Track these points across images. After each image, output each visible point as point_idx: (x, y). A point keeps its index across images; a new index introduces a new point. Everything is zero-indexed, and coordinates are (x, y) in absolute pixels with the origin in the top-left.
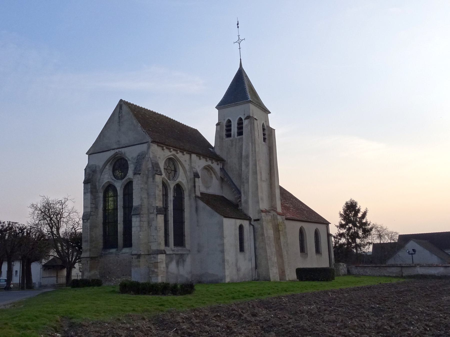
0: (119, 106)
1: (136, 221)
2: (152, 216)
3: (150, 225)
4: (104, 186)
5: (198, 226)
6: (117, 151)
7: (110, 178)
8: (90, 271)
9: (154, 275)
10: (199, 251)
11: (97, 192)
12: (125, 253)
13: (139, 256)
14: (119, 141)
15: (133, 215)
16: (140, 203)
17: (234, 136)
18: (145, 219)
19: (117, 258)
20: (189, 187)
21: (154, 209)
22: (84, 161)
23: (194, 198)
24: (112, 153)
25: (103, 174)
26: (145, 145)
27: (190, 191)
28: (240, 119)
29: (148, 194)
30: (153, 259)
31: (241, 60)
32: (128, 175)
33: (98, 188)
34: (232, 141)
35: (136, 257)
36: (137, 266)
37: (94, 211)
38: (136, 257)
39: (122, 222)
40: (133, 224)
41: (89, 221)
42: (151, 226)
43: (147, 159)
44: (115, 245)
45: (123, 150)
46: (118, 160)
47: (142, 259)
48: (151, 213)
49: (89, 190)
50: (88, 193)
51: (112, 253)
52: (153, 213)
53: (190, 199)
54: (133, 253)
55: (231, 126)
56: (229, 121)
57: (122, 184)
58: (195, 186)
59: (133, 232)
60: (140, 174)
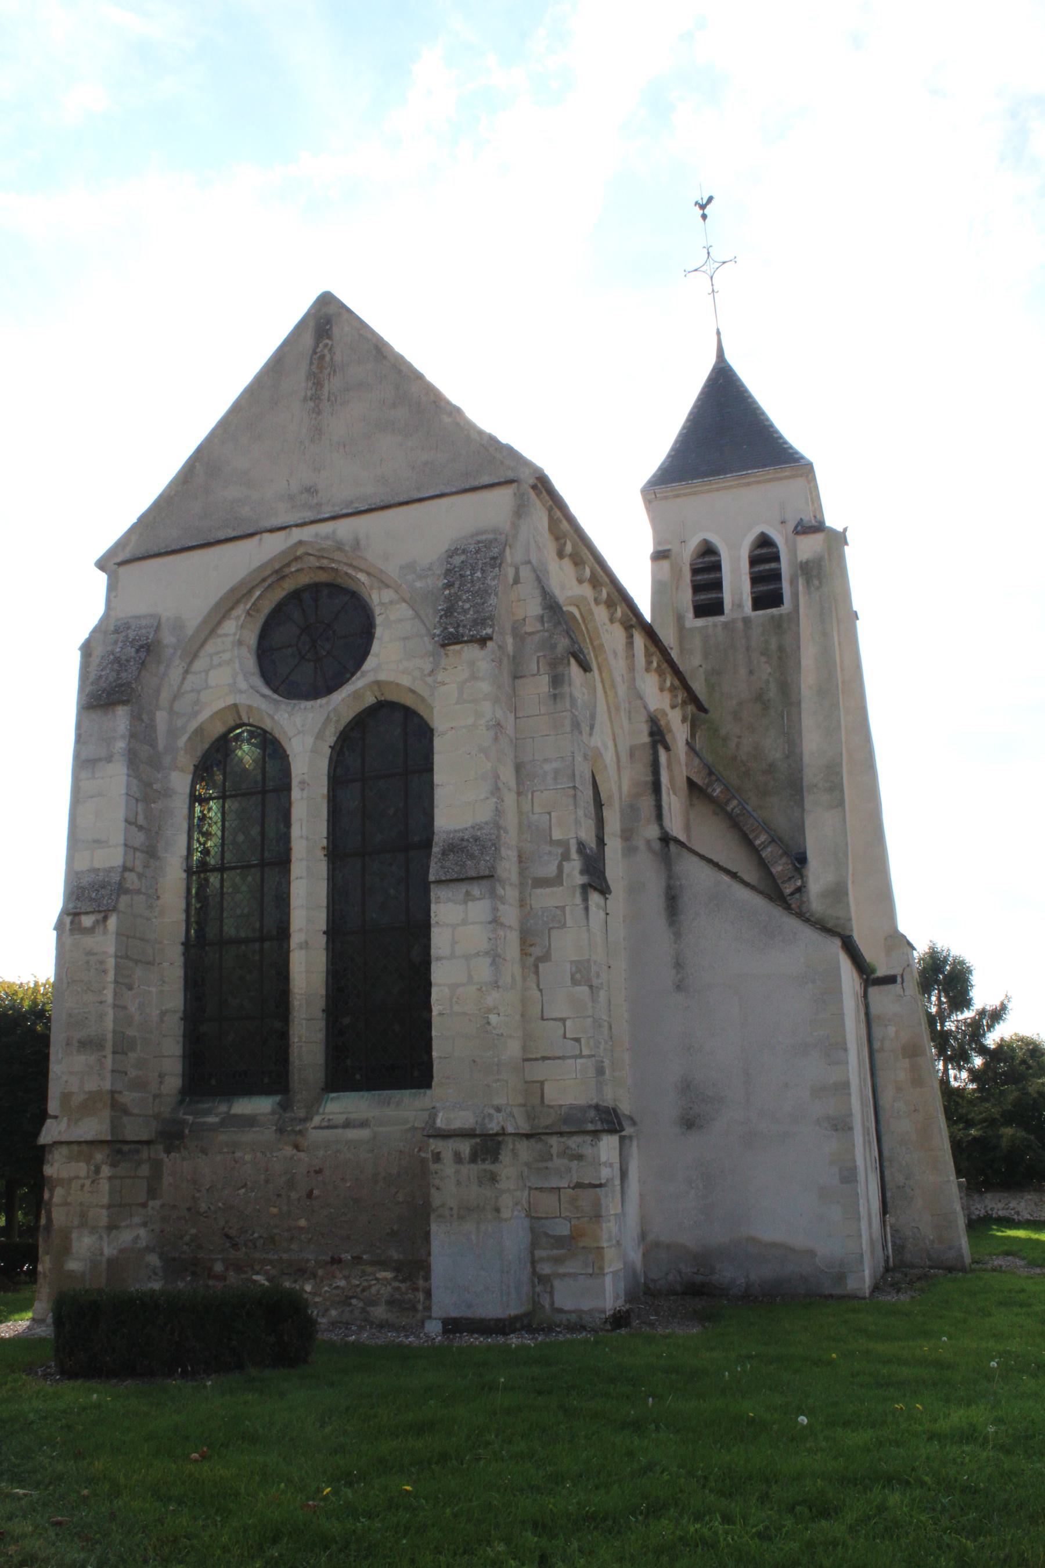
0: (312, 324)
1: (464, 922)
2: (546, 899)
3: (537, 951)
4: (199, 731)
5: (679, 987)
6: (298, 535)
7: (243, 685)
8: (112, 1227)
9: (570, 1267)
10: (689, 1123)
11: (155, 762)
12: (347, 1125)
13: (487, 1145)
14: (311, 490)
15: (439, 882)
16: (484, 814)
17: (740, 606)
18: (510, 914)
19: (289, 1151)
20: (625, 788)
21: (566, 857)
22: (84, 603)
23: (657, 845)
24: (272, 546)
25: (198, 665)
26: (504, 496)
27: (631, 812)
28: (764, 542)
29: (518, 768)
30: (558, 1162)
31: (718, 333)
32: (370, 663)
33: (161, 744)
34: (726, 625)
35: (465, 1147)
36: (467, 1211)
37: (139, 869)
38: (465, 1147)
39: (323, 940)
40: (440, 940)
41: (112, 922)
42: (546, 957)
43: (511, 572)
44: (271, 1073)
45: (344, 529)
46: (296, 595)
47: (508, 1169)
48: (542, 883)
49: (121, 745)
50: (109, 759)
51: (250, 1121)
52: (557, 880)
53: (630, 851)
54: (439, 1123)
55: (717, 567)
56: (708, 550)
57: (328, 719)
58: (656, 787)
59: (437, 994)
60: (483, 641)
